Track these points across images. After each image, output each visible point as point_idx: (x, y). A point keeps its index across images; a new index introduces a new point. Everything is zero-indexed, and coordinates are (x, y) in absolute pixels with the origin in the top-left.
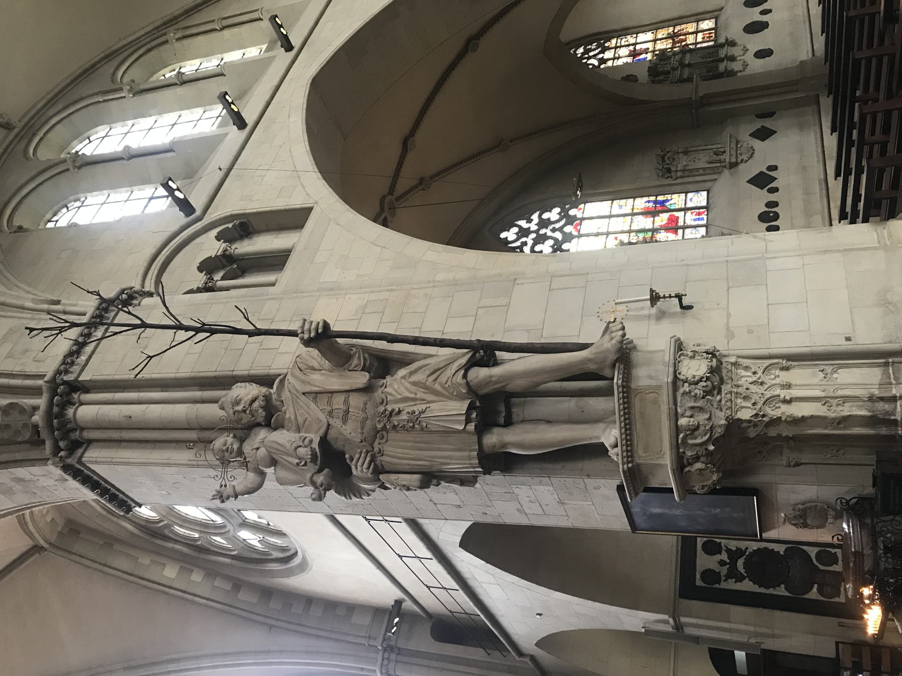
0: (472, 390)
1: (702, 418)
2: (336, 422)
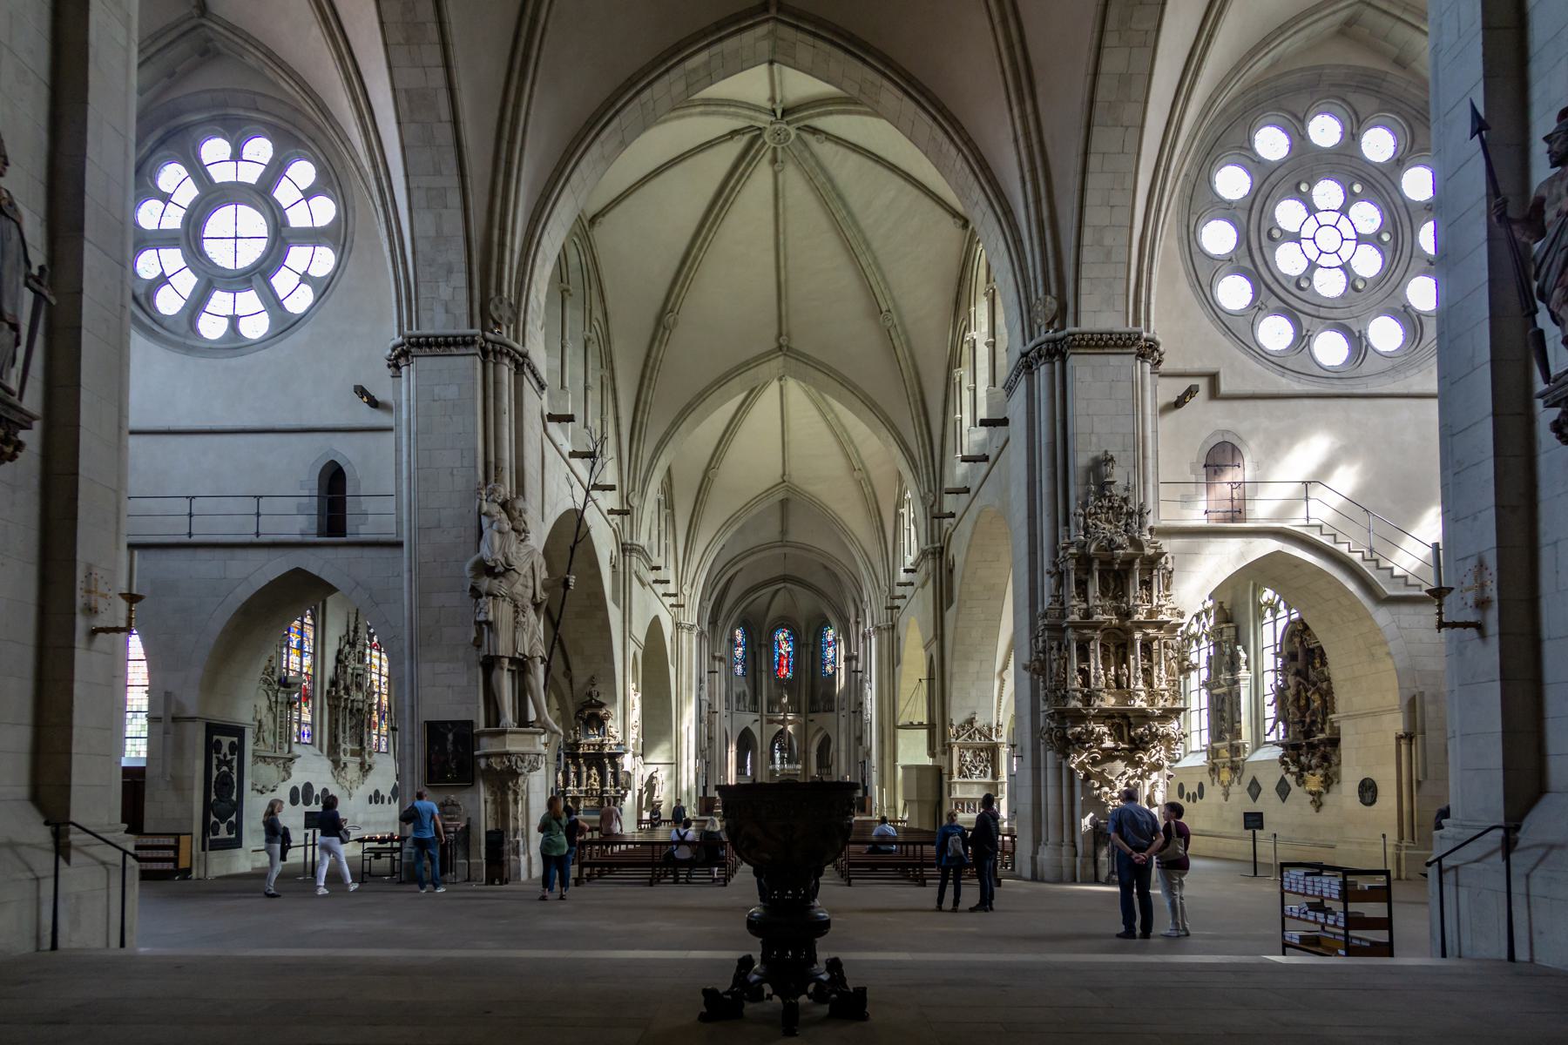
0: (532, 658)
2: (522, 580)
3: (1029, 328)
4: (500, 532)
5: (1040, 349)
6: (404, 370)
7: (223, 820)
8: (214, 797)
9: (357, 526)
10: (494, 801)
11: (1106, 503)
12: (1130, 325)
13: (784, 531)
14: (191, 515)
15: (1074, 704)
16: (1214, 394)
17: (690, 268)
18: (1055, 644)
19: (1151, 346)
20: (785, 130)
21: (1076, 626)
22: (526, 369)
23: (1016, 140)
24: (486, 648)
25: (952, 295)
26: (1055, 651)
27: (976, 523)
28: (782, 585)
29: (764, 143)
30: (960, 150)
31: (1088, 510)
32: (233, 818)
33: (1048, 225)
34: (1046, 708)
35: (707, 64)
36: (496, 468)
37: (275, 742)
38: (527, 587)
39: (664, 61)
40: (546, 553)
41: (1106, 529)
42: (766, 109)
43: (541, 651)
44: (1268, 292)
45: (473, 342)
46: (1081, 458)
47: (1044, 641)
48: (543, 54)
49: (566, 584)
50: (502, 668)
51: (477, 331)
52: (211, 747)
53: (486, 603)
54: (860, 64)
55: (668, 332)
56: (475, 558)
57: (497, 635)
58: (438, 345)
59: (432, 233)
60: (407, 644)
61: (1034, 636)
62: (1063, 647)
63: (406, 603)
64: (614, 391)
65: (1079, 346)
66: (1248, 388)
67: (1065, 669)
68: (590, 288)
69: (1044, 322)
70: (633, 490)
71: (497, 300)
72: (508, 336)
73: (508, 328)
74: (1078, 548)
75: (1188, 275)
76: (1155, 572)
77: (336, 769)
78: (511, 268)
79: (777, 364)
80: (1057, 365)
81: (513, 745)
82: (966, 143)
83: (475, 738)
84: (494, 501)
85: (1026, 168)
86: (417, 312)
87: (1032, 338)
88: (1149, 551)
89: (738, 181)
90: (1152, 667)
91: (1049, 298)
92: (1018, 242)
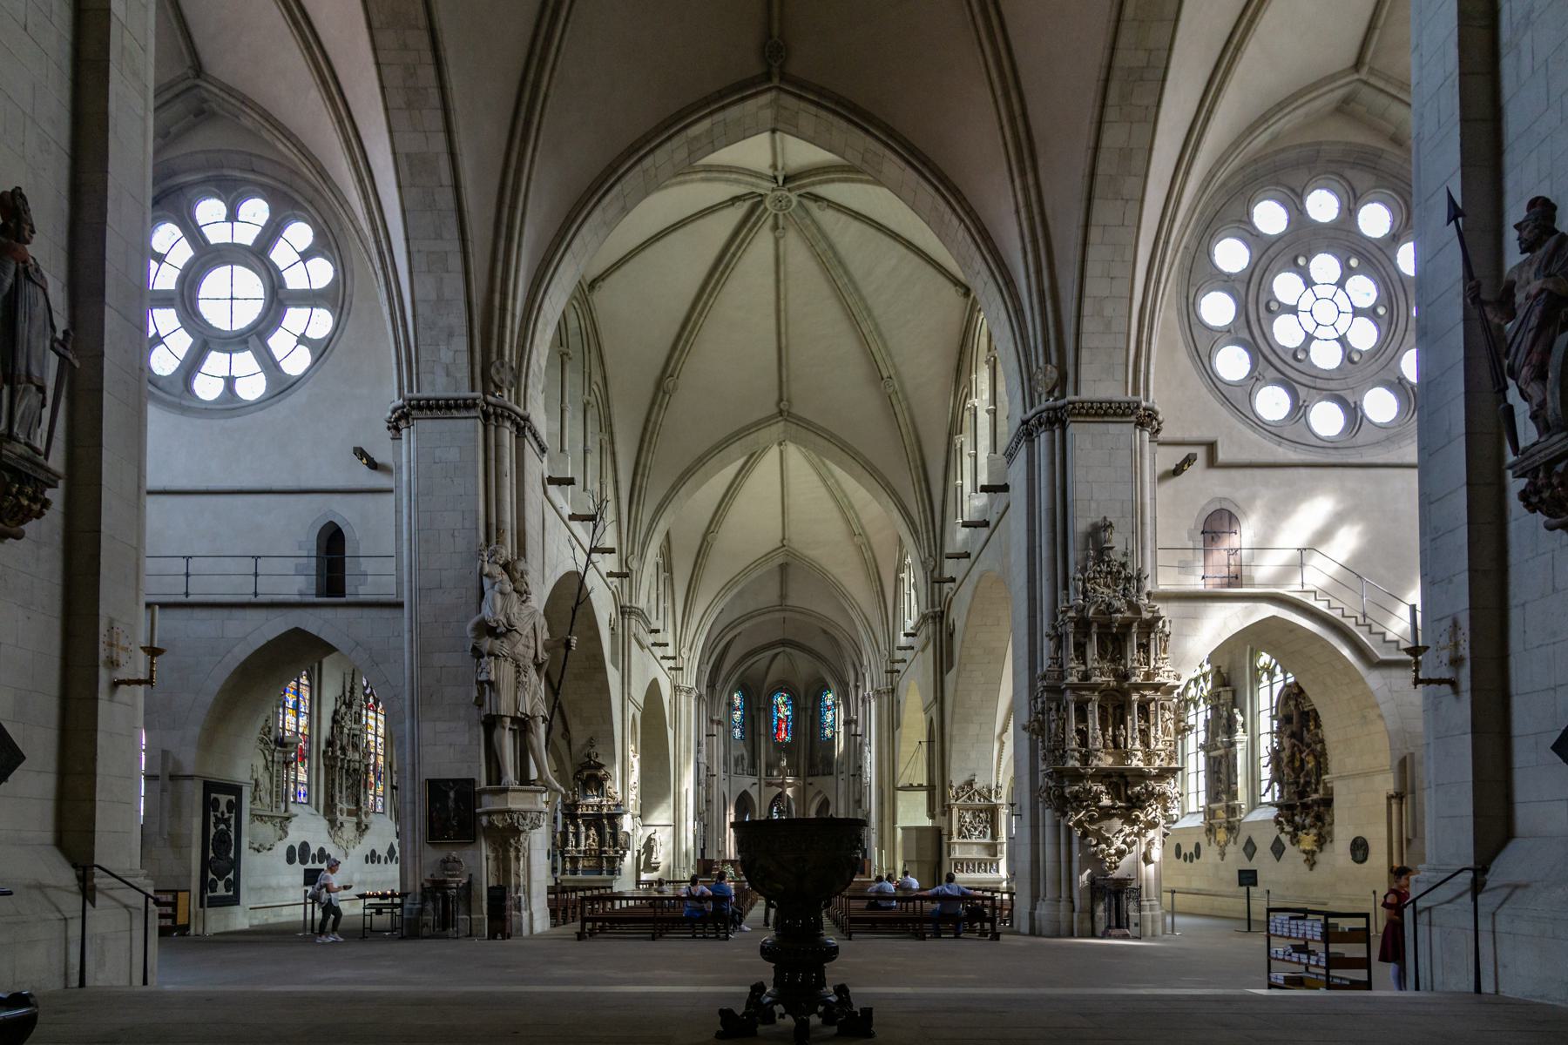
0: (534, 717)
1: (528, 821)
2: (523, 640)
3: (1030, 397)
4: (502, 593)
5: (1040, 417)
6: (404, 432)
7: (220, 877)
8: (211, 855)
9: (356, 587)
10: (496, 858)
11: (1104, 568)
12: (1130, 395)
13: (783, 596)
14: (187, 575)
15: (1073, 763)
16: (1212, 462)
17: (691, 333)
18: (1054, 705)
19: (1149, 415)
20: (787, 197)
21: (1075, 688)
22: (527, 433)
23: (1017, 212)
24: (488, 707)
25: (953, 362)
26: (1053, 712)
27: (976, 587)
28: (782, 649)
29: (766, 209)
30: (962, 220)
31: (1086, 575)
32: (231, 876)
33: (1050, 295)
34: (1044, 767)
35: (710, 131)
36: (498, 530)
37: (271, 802)
38: (528, 647)
39: (667, 128)
40: (547, 613)
41: (1104, 593)
42: (767, 176)
43: (543, 710)
44: (1266, 363)
45: (475, 405)
46: (1080, 524)
47: (1043, 703)
48: (545, 121)
49: (568, 645)
50: (504, 728)
51: (478, 394)
52: (209, 805)
53: (488, 663)
54: (862, 134)
55: (668, 396)
56: (476, 619)
57: (498, 692)
58: (439, 408)
59: (433, 296)
60: (407, 703)
61: (1033, 698)
62: (1061, 708)
63: (407, 662)
64: (614, 454)
65: (1079, 414)
66: (1245, 457)
67: (1064, 729)
68: (589, 352)
69: (1044, 391)
70: (632, 553)
71: (498, 363)
72: (510, 399)
73: (509, 391)
74: (1077, 612)
75: (1187, 345)
76: (1152, 636)
77: (332, 828)
78: (512, 332)
79: (777, 429)
80: (1057, 432)
81: (515, 802)
82: (967, 214)
83: (477, 796)
84: (496, 563)
85: (1027, 239)
86: (417, 374)
87: (1032, 406)
88: (1146, 615)
89: (739, 247)
90: (1149, 728)
91: (1049, 367)
92: (1019, 311)
